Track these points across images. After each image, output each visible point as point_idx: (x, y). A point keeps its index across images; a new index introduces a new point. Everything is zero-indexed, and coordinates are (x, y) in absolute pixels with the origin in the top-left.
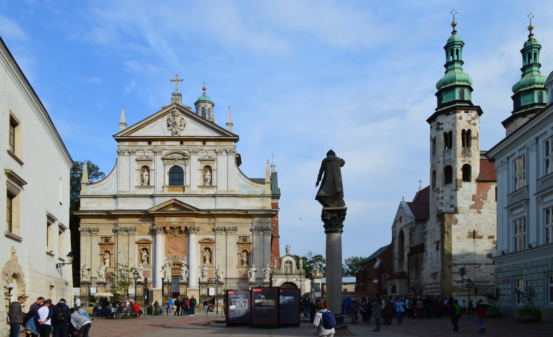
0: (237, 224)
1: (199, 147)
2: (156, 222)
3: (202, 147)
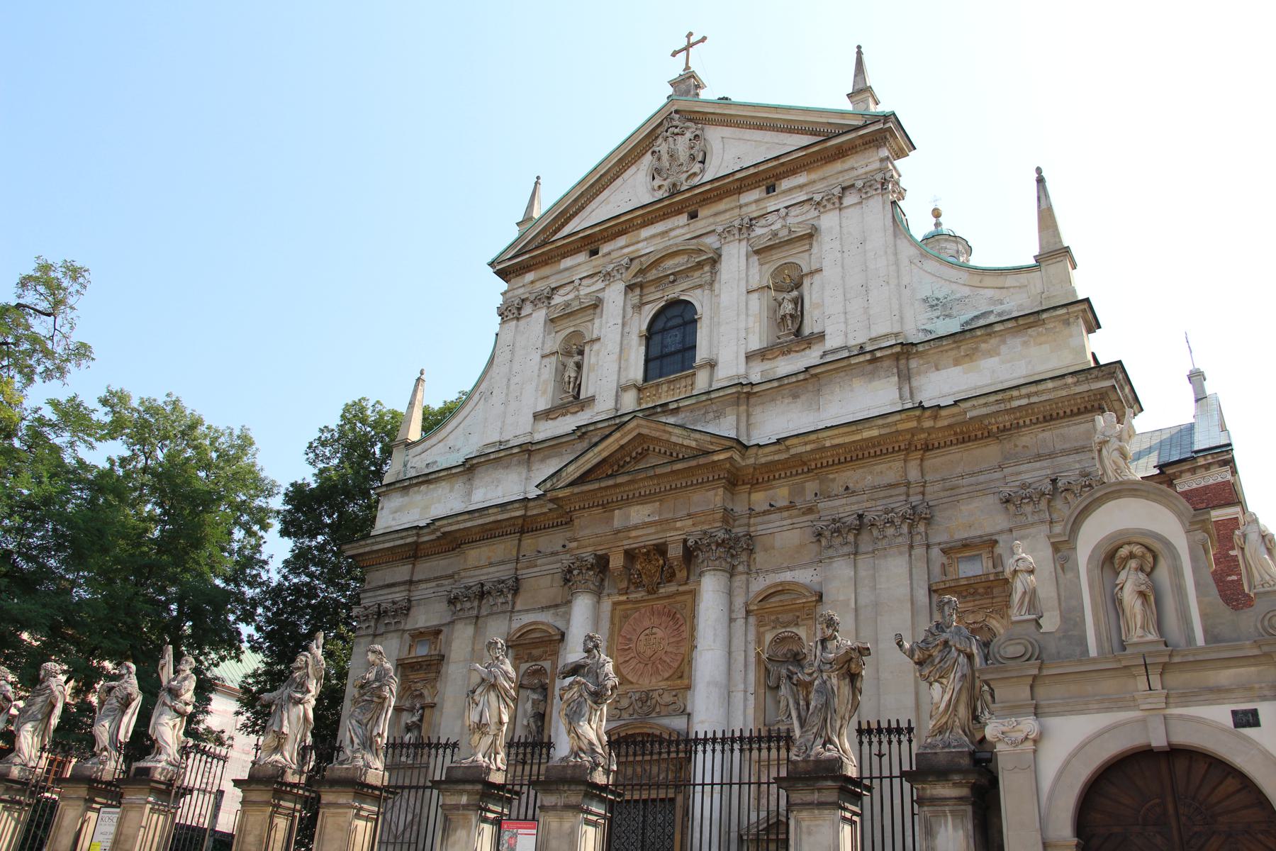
0: (929, 489)
1: (754, 207)
3: (762, 205)
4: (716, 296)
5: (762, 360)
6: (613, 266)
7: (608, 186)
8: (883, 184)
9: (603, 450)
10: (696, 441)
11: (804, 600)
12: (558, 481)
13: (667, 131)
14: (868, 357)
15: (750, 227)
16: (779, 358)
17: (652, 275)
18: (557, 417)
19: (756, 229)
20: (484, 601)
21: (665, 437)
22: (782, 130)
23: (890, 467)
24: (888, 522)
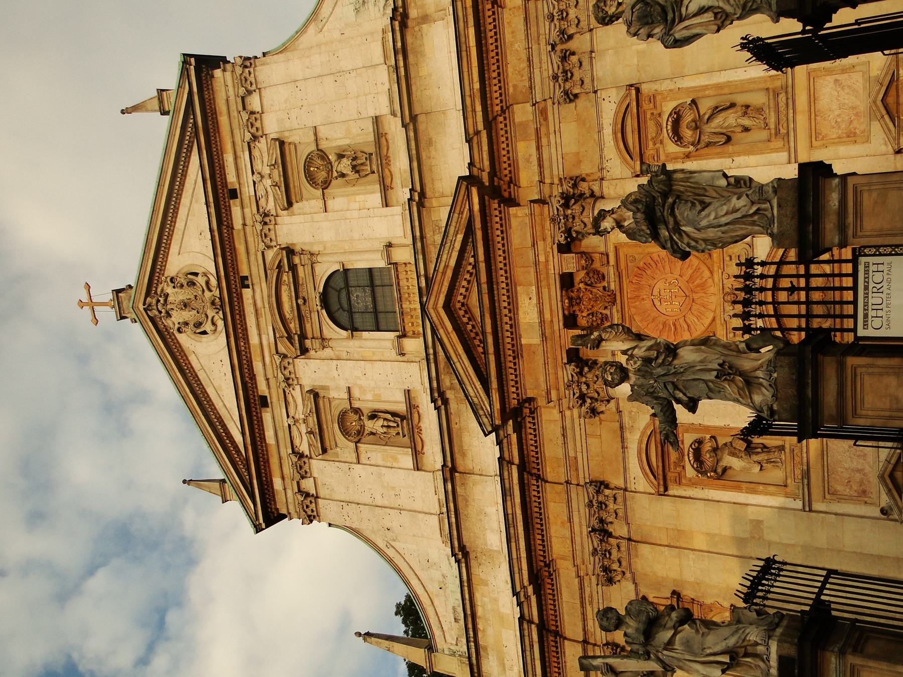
1: (247, 211)
2: (548, 393)
3: (246, 202)
4: (325, 249)
5: (392, 188)
6: (280, 374)
7: (203, 388)
8: (246, 67)
9: (455, 351)
10: (457, 233)
11: (635, 103)
12: (483, 410)
13: (160, 312)
14: (400, 58)
15: (266, 215)
16: (393, 168)
17: (294, 326)
18: (422, 441)
19: (268, 209)
20: (611, 529)
21: (449, 273)
22: (182, 184)
23: (508, 23)
24: (562, 14)
